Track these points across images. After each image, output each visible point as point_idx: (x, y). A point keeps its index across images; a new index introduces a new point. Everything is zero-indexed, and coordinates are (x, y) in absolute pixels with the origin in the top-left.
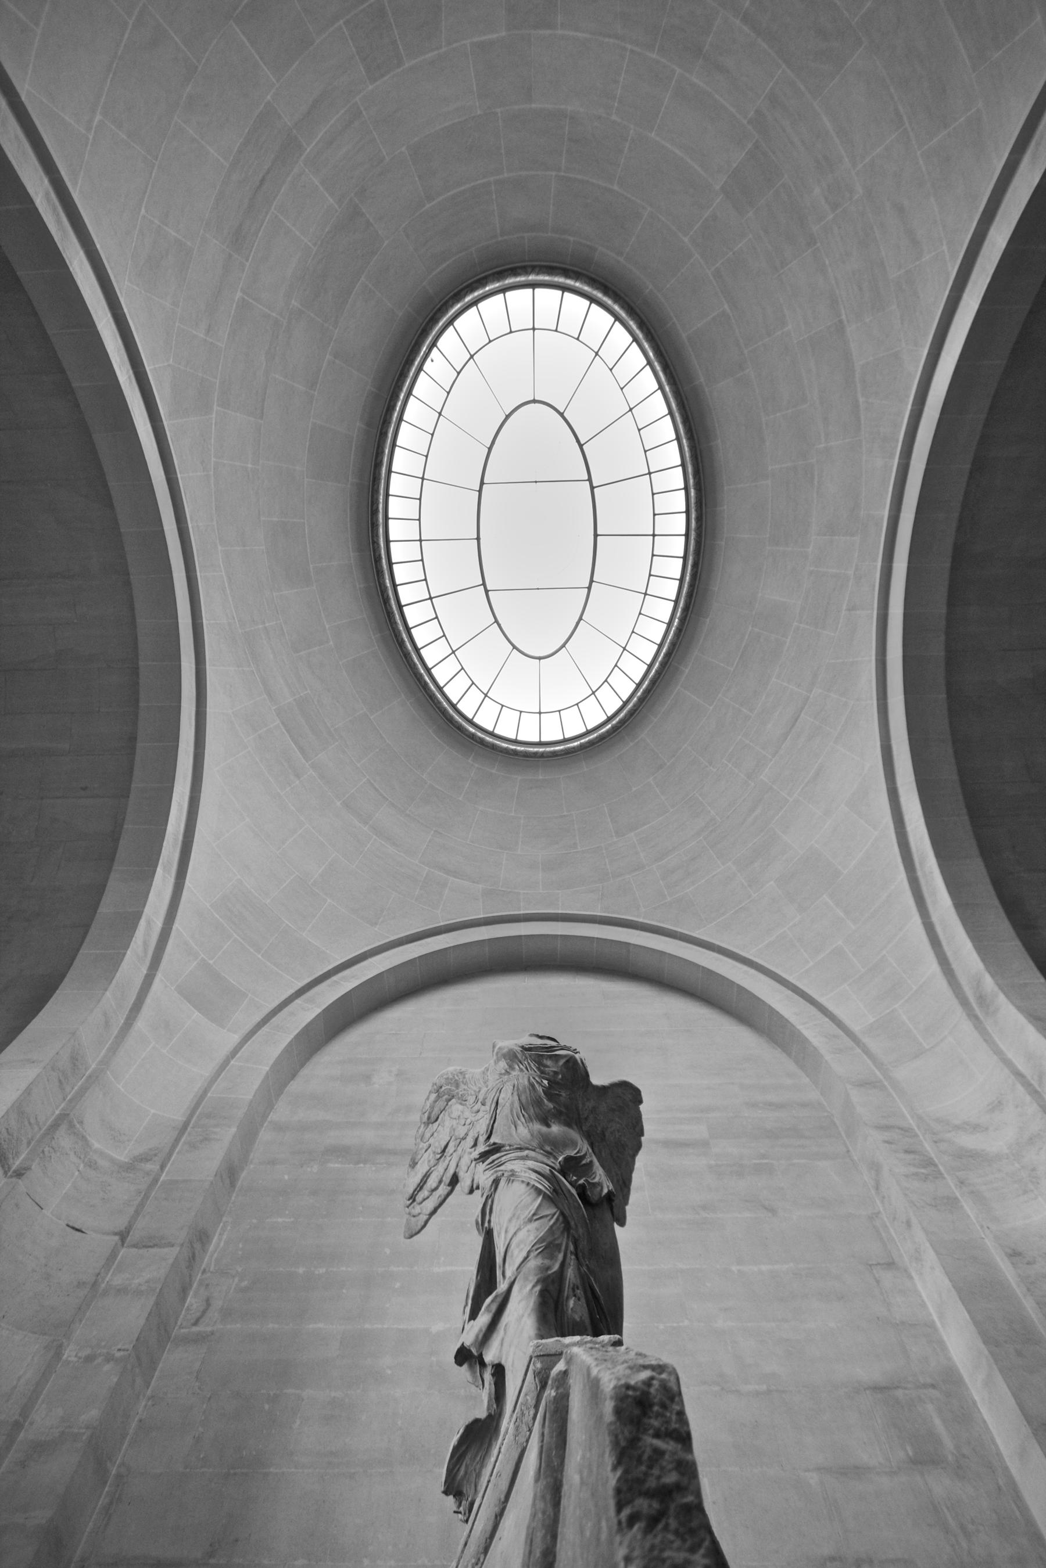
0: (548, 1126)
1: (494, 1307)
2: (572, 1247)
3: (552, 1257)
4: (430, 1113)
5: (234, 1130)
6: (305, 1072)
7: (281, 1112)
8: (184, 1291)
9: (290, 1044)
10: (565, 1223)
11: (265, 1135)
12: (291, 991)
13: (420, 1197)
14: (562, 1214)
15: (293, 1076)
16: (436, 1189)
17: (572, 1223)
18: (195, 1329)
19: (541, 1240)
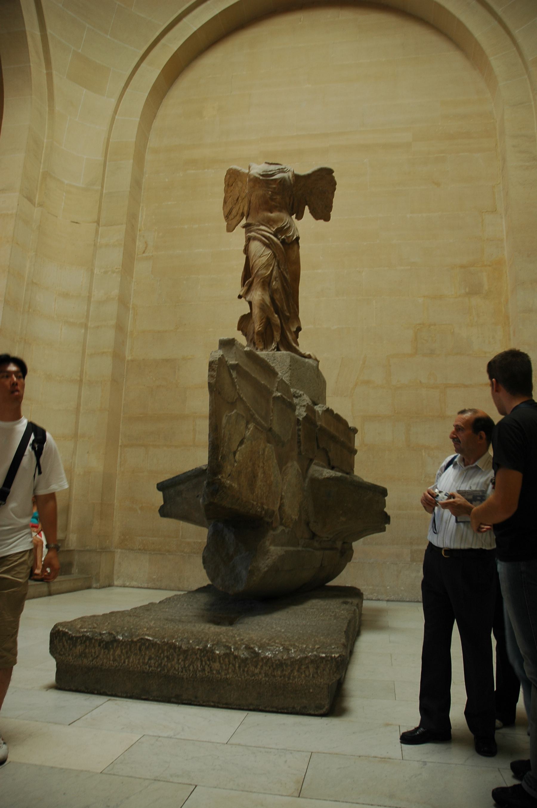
0: (272, 213)
1: (249, 285)
2: (276, 264)
3: (268, 269)
4: (229, 182)
5: (131, 161)
6: (161, 112)
7: (153, 142)
8: (134, 241)
9: (147, 100)
10: (275, 256)
11: (148, 157)
12: (137, 59)
13: (231, 217)
14: (273, 252)
15: (155, 117)
16: (236, 216)
17: (277, 255)
18: (144, 255)
19: (264, 264)
